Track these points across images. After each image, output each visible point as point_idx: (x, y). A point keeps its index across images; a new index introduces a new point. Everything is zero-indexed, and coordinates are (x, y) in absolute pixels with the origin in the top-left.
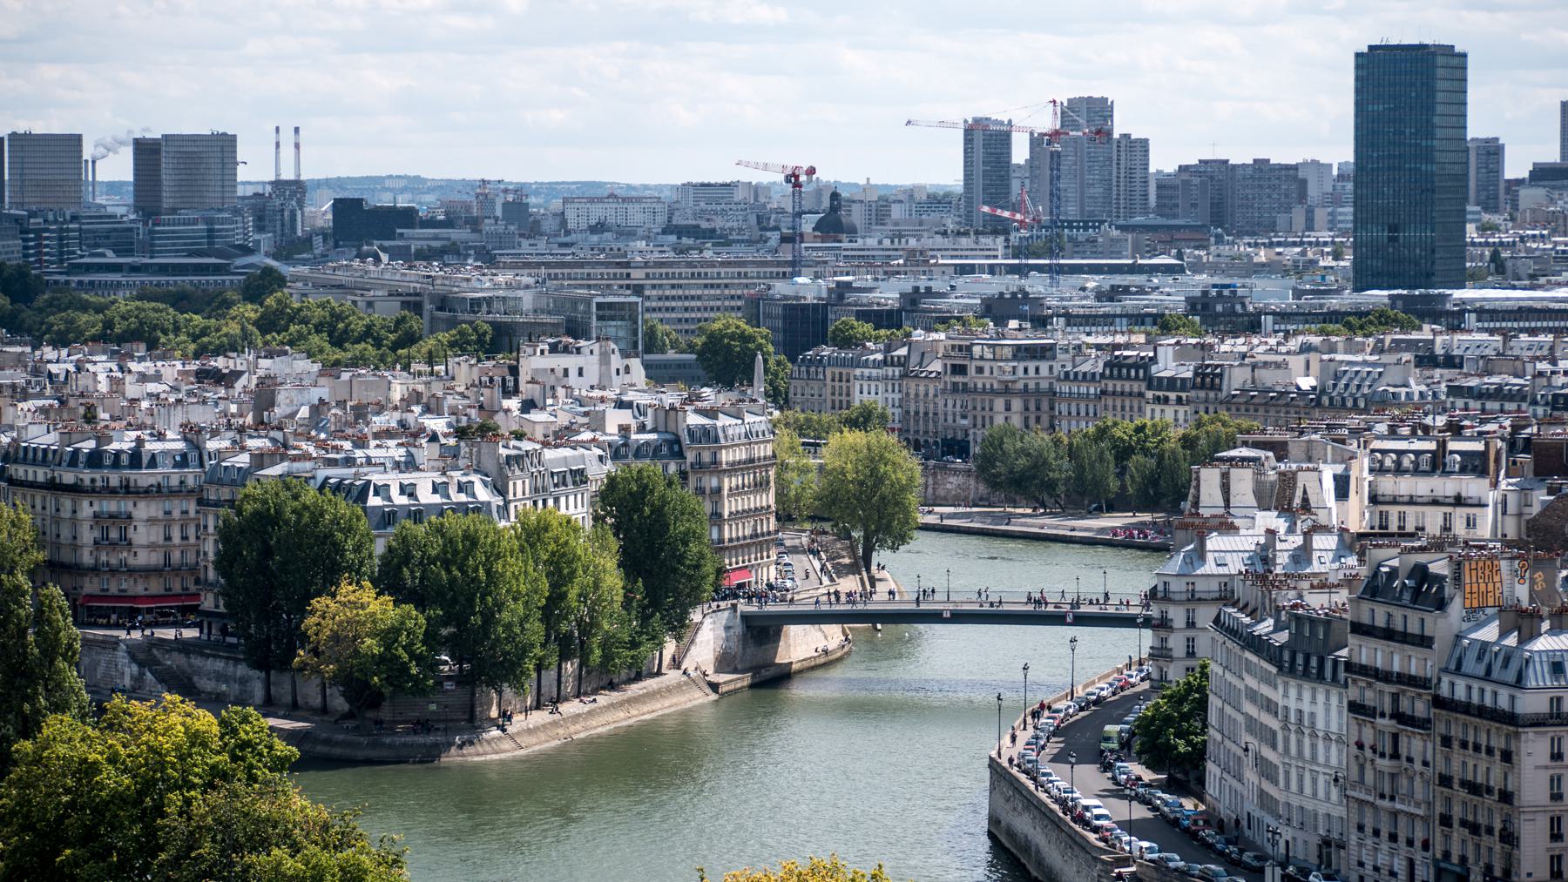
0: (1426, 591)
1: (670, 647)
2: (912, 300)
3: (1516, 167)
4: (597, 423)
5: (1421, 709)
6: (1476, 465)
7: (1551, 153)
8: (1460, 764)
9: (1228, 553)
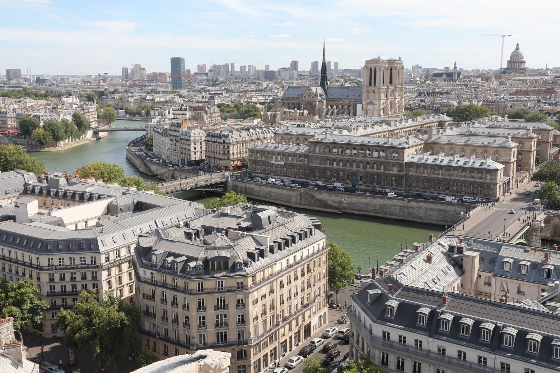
0: (179, 125)
1: (83, 135)
2: (116, 90)
3: (192, 73)
4: (72, 107)
5: (179, 140)
6: (186, 110)
8: (184, 146)
9: (154, 121)
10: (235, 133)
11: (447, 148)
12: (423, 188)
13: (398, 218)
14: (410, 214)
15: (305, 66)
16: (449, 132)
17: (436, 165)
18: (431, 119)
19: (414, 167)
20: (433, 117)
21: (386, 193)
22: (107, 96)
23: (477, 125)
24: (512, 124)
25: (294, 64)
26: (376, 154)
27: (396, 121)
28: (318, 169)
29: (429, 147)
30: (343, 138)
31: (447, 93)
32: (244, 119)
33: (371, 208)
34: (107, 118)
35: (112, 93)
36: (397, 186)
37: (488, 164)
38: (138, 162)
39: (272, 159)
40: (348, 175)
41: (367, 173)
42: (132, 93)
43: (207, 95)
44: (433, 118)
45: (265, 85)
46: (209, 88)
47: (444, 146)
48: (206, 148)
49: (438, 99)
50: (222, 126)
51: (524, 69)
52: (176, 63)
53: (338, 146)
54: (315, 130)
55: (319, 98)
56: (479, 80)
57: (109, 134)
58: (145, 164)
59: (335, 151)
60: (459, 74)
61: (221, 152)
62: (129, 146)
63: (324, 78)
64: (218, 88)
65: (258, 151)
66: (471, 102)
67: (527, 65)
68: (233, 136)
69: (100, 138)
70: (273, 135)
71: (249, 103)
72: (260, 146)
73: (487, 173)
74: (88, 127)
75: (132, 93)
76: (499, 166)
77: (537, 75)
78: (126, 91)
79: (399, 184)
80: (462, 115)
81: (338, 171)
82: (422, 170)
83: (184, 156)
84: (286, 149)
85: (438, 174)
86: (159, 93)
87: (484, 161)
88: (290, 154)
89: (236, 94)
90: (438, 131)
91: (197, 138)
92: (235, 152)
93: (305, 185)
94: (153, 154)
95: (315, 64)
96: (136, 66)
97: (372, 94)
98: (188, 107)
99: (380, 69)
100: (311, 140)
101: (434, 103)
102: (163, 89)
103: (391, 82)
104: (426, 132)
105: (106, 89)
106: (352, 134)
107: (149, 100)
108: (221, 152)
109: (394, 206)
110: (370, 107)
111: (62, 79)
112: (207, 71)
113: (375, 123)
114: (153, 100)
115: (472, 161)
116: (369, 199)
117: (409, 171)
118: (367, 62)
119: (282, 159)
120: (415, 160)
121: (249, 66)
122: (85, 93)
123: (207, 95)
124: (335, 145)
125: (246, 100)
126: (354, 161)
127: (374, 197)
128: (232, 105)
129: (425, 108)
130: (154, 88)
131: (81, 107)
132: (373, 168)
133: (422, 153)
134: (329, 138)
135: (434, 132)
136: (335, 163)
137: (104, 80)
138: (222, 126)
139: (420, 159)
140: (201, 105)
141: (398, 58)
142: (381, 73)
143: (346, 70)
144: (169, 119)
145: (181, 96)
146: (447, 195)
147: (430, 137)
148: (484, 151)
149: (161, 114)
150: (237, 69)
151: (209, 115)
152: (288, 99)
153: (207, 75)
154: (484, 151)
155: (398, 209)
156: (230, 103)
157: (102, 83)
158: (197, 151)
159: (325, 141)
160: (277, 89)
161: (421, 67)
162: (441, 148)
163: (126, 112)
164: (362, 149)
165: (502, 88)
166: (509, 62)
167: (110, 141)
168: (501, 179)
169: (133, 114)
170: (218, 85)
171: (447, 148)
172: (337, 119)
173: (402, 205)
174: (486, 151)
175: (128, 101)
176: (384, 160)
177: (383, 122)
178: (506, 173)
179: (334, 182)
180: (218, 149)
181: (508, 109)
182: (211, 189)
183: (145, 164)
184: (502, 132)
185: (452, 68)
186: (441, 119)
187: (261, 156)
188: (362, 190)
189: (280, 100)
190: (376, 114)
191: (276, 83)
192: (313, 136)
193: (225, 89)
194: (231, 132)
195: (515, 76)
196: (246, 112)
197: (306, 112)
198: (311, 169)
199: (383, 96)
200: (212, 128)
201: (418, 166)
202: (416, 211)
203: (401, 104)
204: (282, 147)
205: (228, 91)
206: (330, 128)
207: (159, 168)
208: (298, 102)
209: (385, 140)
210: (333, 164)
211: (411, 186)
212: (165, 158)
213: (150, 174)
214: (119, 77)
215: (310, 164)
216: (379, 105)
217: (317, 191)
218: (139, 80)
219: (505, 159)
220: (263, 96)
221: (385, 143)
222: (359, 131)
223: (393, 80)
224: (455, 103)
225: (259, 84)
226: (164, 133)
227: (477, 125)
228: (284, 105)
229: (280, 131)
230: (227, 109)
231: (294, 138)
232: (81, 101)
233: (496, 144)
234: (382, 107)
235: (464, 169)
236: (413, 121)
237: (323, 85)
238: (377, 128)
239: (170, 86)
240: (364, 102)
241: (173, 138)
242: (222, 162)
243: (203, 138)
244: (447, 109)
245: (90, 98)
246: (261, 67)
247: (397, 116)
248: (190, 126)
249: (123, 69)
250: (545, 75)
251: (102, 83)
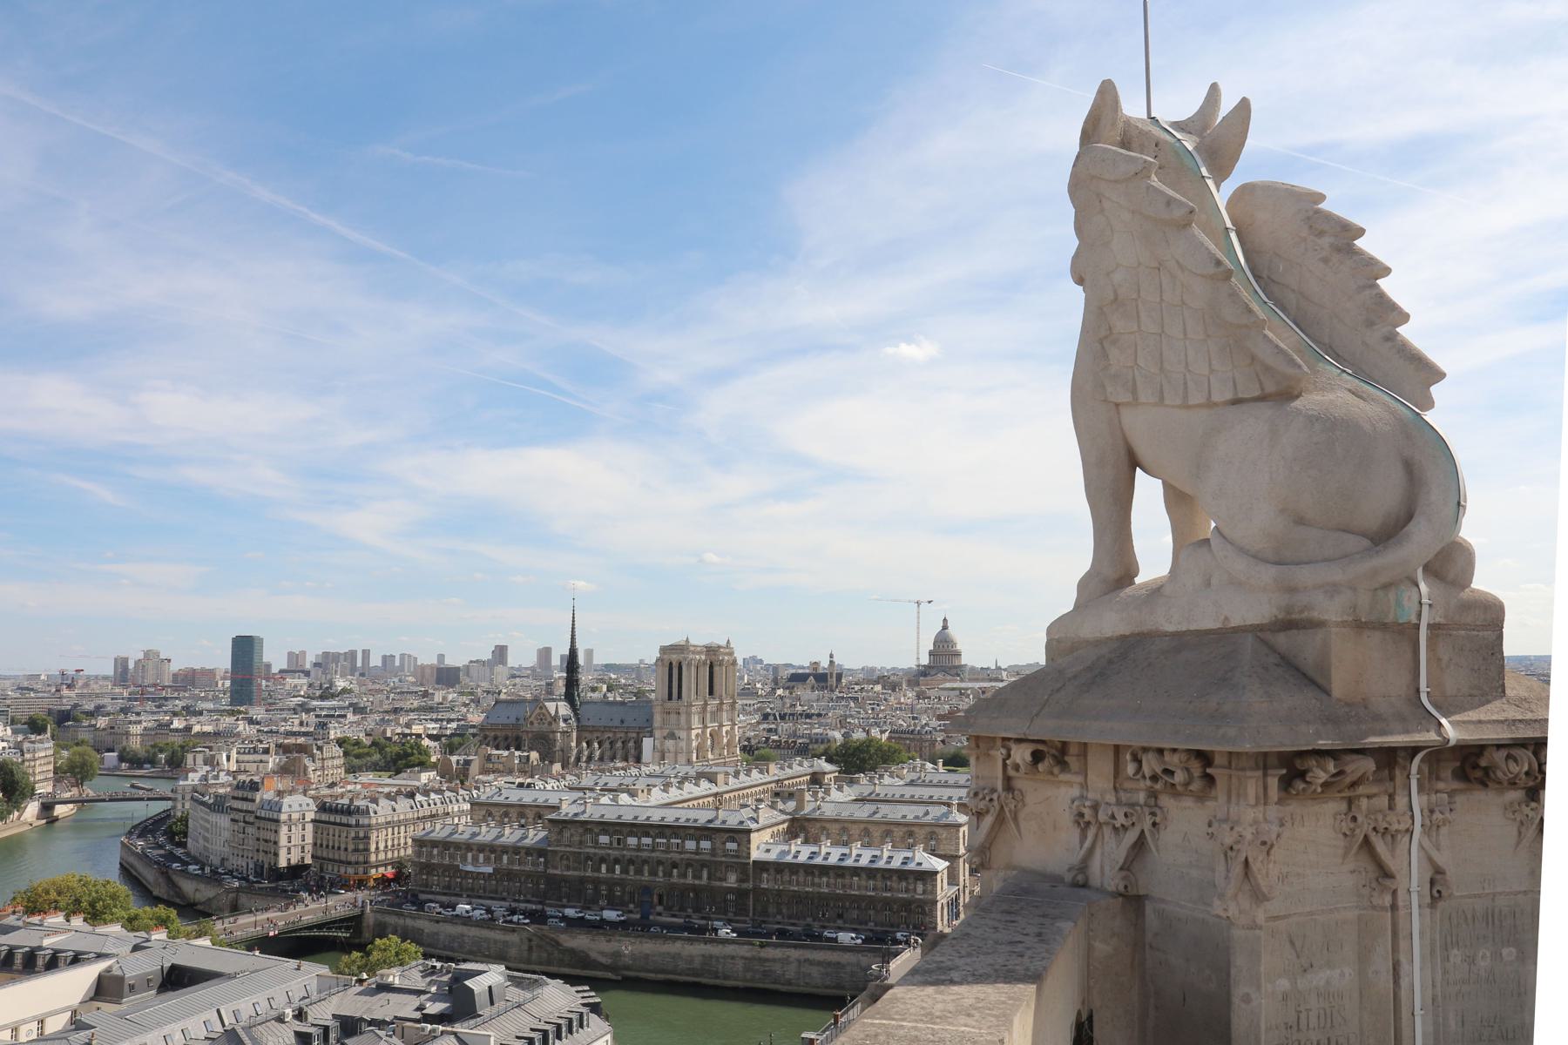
0: (254, 787)
2: (98, 708)
3: (275, 670)
5: (252, 820)
6: (266, 751)
7: (285, 667)
8: (263, 834)
9: (194, 778)
10: (383, 802)
11: (834, 828)
12: (790, 917)
13: (740, 984)
14: (766, 974)
15: (522, 656)
16: (835, 795)
17: (815, 866)
18: (797, 769)
19: (772, 871)
20: (801, 765)
21: (716, 930)
22: (76, 720)
23: (887, 780)
24: (952, 778)
25: (501, 653)
26: (690, 845)
27: (727, 774)
28: (564, 879)
29: (799, 827)
30: (622, 811)
31: (819, 715)
32: (398, 772)
33: (682, 965)
34: (74, 772)
35: (91, 714)
36: (735, 914)
37: (917, 860)
38: (149, 875)
39: (464, 859)
40: (632, 894)
41: (673, 887)
42: (138, 714)
43: (311, 719)
44: (800, 768)
45: (438, 698)
46: (315, 703)
47: (828, 825)
48: (315, 838)
49: (803, 728)
50: (349, 787)
51: (961, 666)
52: (245, 648)
53: (611, 829)
54: (555, 791)
55: (562, 724)
56: (878, 688)
59: (604, 839)
60: (839, 677)
61: (351, 847)
62: (130, 833)
63: (572, 683)
64: (334, 703)
65: (435, 844)
66: (868, 732)
67: (964, 660)
68: (379, 809)
69: (56, 819)
70: (467, 806)
71: (405, 735)
72: (439, 831)
73: (916, 879)
74: (30, 793)
75: (138, 714)
76: (940, 865)
77: (983, 680)
78: (125, 711)
79: (742, 910)
80: (855, 760)
81: (611, 884)
82: (786, 878)
83: (261, 856)
84: (498, 837)
85: (819, 886)
86: (201, 713)
87: (909, 854)
88: (505, 849)
89: (377, 717)
90: (815, 794)
91: (295, 816)
92: (382, 846)
93: (538, 918)
94: (188, 854)
95: (545, 654)
96: (147, 654)
97: (673, 717)
98: (273, 746)
99: (689, 665)
100: (553, 816)
101: (794, 734)
102: (211, 706)
103: (711, 692)
104: (791, 795)
105: (76, 706)
106: (639, 801)
107: (177, 730)
108: (351, 847)
109: (733, 958)
110: (670, 743)
112: (308, 666)
113: (685, 779)
114: (188, 729)
115: (886, 854)
116: (678, 944)
117: (761, 881)
118: (664, 650)
119: (487, 861)
120: (772, 857)
121: (402, 656)
122: (24, 714)
123: (311, 719)
124: (605, 827)
125: (399, 730)
126: (645, 861)
127: (689, 939)
128: (366, 741)
129: (778, 745)
130: (189, 702)
131: (18, 746)
132: (685, 876)
133: (787, 841)
134: (592, 813)
135: (808, 797)
136: (604, 868)
137: (69, 687)
138: (349, 787)
139: (783, 853)
140: (301, 740)
141: (723, 643)
142: (690, 673)
143: (609, 667)
144: (229, 773)
145: (251, 721)
146: (841, 929)
147: (800, 806)
148: (907, 834)
149: (211, 762)
150: (376, 661)
151: (319, 764)
152: (494, 727)
153: (307, 674)
154: (907, 834)
155: (740, 964)
156: (362, 735)
158: (294, 845)
159: (582, 818)
160: (465, 705)
161: (761, 661)
162: (824, 828)
163: (121, 759)
164: (662, 835)
165: (923, 704)
166: (931, 653)
167: (78, 825)
168: (944, 892)
169: (135, 761)
170: (333, 696)
171: (834, 828)
172: (603, 771)
173: (748, 955)
174: (911, 834)
175: (127, 734)
176: (707, 858)
177: (700, 776)
178: (953, 879)
179: (602, 909)
180: (343, 839)
181: (939, 746)
182: (316, 933)
184: (937, 793)
185: (825, 664)
186: (816, 769)
187: (441, 854)
188: (663, 926)
189: (471, 731)
190: (682, 758)
191: (462, 694)
192: (556, 808)
193: (351, 705)
194: (375, 801)
195: (946, 681)
196: (402, 758)
197: (534, 755)
198: (552, 881)
199: (696, 721)
200: (326, 792)
201: (778, 868)
202: (777, 968)
203: (733, 736)
204: (487, 833)
205: (357, 709)
206: (592, 790)
207: (202, 886)
208: (516, 732)
209: (710, 815)
210: (599, 870)
211: (765, 913)
212: (216, 861)
213: (178, 901)
214: (106, 678)
215: (551, 871)
216: (689, 740)
217: (564, 931)
218: (155, 685)
219: (950, 851)
220: (436, 721)
221: (710, 821)
222: (652, 795)
223: (716, 688)
224: (838, 735)
225: (426, 694)
226: (218, 805)
227: (887, 780)
228: (485, 741)
229: (483, 798)
230: (357, 751)
231: (513, 813)
232: (15, 732)
233: (928, 819)
234: (694, 744)
235: (871, 873)
236: (761, 772)
237: (570, 697)
238: (690, 789)
239: (225, 700)
240: (657, 734)
241: (240, 816)
242: (350, 870)
243: (310, 816)
244: (822, 747)
245: (35, 727)
246: (427, 659)
247: (725, 764)
248: (280, 787)
250: (997, 680)
251: (65, 692)
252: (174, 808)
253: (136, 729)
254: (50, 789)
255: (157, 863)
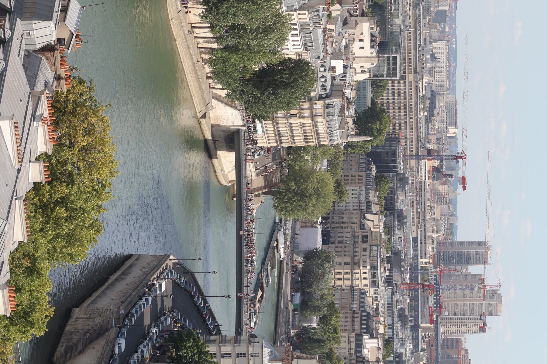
1: (223, 93)
2: (400, 217)
4: (336, 55)
22: (379, 181)
34: (289, 179)
35: (388, 205)
38: (108, 301)
42: (389, 281)
57: (227, 189)
58: (99, 332)
62: (181, 269)
69: (210, 154)
74: (256, 111)
75: (389, 281)
78: (395, 258)
96: (493, 296)
105: (403, 180)
107: (359, 346)
111: (441, 17)
131: (337, 90)
137: (437, 170)
157: (428, 164)
163: (311, 256)
175: (355, 264)
183: (99, 332)
213: (61, 349)
214: (451, 229)
218: (439, 307)
232: (359, 86)
245: (369, 119)
249: (483, 244)
251: (428, 164)
252: (223, 341)
253: (362, 279)
254: (262, 142)
255: (128, 315)
